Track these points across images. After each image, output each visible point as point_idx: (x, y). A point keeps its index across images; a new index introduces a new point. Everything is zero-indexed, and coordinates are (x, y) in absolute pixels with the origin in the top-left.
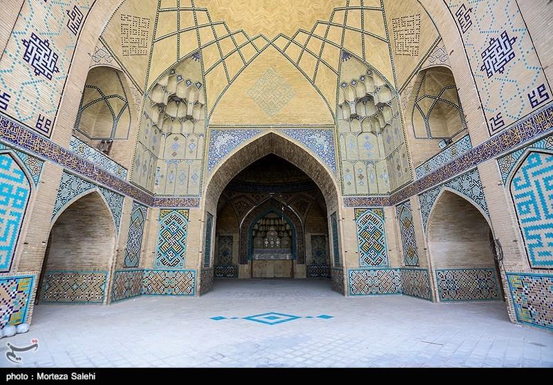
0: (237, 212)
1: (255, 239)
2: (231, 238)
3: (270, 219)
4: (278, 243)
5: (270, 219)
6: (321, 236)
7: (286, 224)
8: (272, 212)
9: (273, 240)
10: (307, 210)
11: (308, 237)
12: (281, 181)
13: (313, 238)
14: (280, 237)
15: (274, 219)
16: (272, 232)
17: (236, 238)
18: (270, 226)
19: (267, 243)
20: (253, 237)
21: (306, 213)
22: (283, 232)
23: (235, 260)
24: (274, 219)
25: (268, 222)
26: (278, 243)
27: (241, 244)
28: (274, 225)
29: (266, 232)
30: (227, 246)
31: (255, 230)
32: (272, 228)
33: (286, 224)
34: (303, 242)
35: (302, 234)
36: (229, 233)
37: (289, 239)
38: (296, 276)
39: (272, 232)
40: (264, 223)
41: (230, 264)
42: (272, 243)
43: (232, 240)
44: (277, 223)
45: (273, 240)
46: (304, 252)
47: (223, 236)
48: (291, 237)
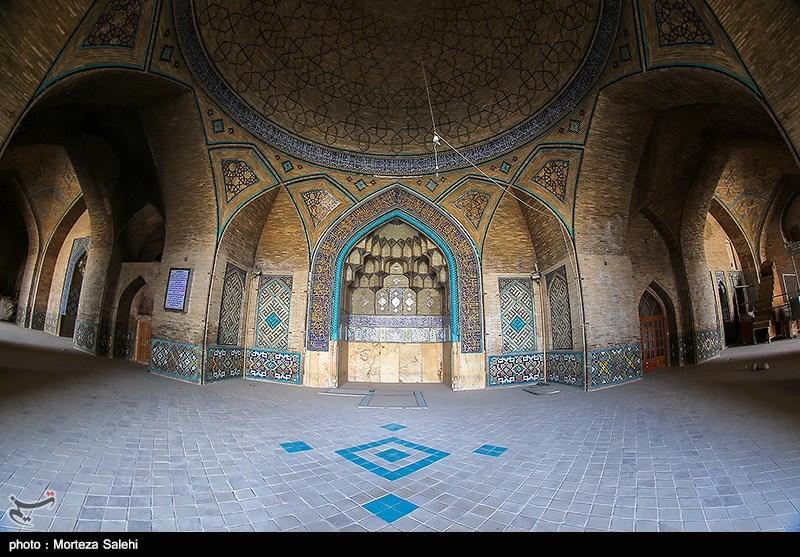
0: (307, 217)
1: (356, 295)
2: (287, 281)
3: (392, 243)
4: (409, 302)
5: (392, 243)
6: (522, 281)
7: (430, 252)
8: (397, 221)
9: (398, 295)
10: (488, 212)
11: (490, 281)
12: (419, 151)
13: (503, 283)
14: (416, 289)
15: (402, 243)
16: (396, 275)
17: (302, 279)
18: (392, 260)
19: (383, 301)
20: (351, 287)
21: (485, 221)
22: (423, 277)
23: (296, 338)
24: (402, 243)
25: (386, 252)
26: (409, 302)
27: (314, 299)
28: (402, 260)
29: (382, 274)
30: (279, 302)
31: (352, 266)
32: (397, 268)
33: (430, 252)
34: (476, 295)
35: (474, 275)
36: (285, 268)
37: (435, 294)
38: (459, 386)
39: (396, 275)
40: (376, 253)
41: (283, 347)
42: (396, 302)
43: (290, 286)
44: (408, 254)
45: (398, 295)
46: (480, 324)
47: (269, 278)
48: (442, 288)
